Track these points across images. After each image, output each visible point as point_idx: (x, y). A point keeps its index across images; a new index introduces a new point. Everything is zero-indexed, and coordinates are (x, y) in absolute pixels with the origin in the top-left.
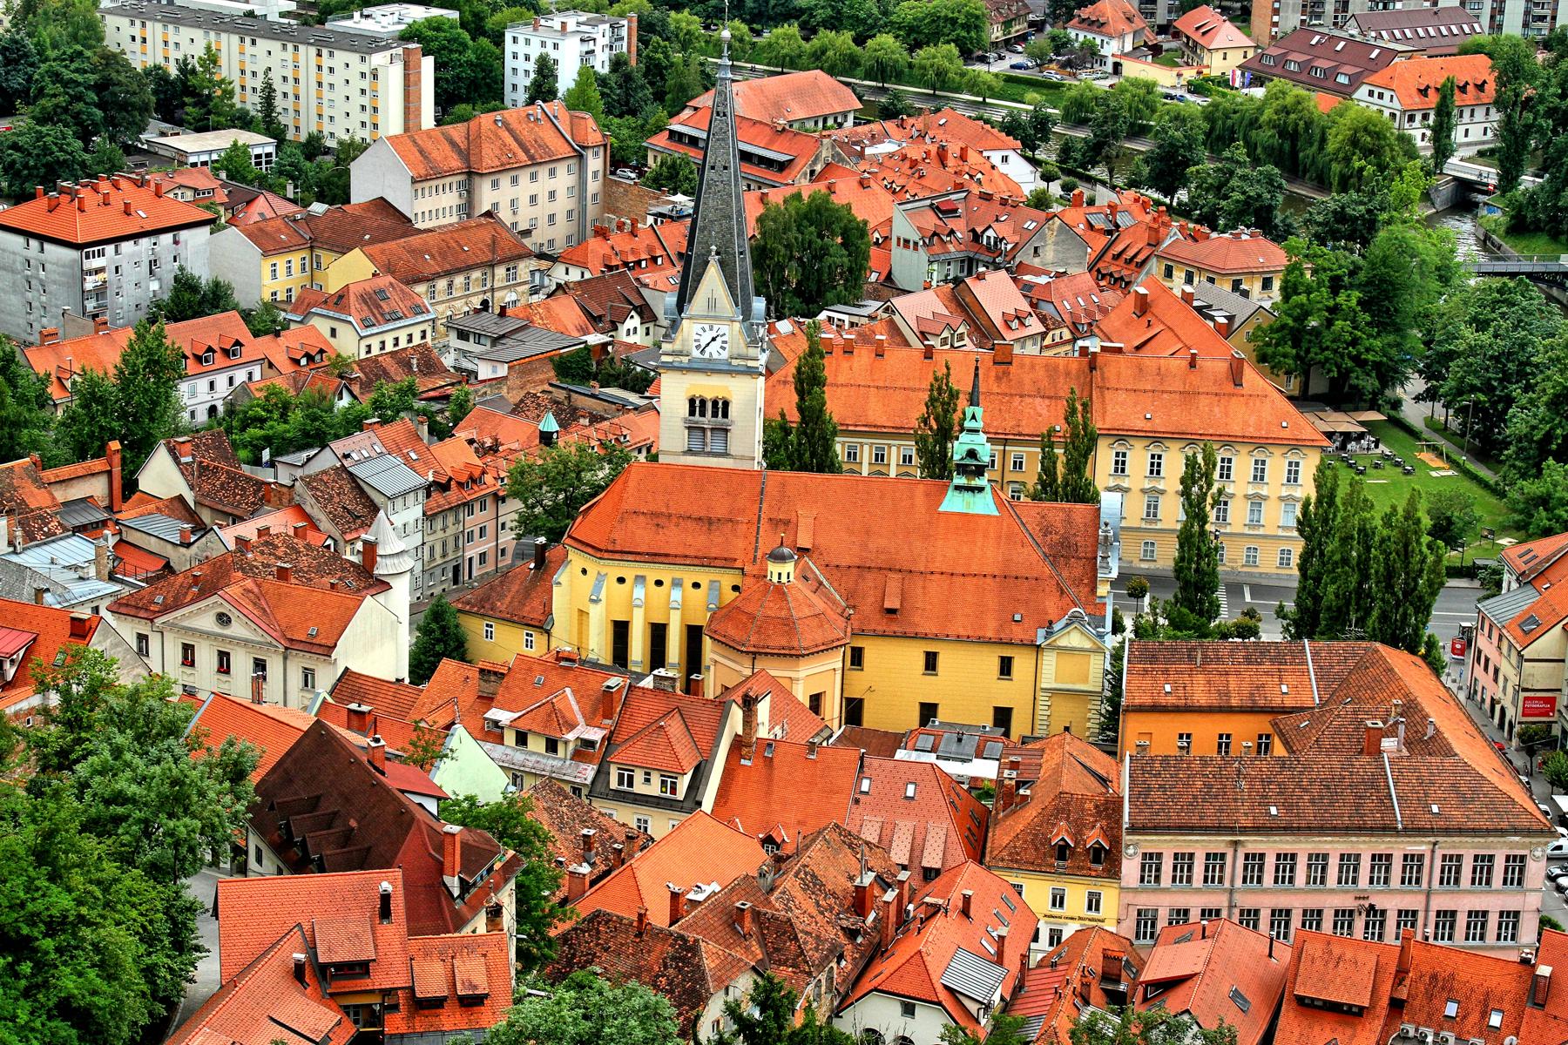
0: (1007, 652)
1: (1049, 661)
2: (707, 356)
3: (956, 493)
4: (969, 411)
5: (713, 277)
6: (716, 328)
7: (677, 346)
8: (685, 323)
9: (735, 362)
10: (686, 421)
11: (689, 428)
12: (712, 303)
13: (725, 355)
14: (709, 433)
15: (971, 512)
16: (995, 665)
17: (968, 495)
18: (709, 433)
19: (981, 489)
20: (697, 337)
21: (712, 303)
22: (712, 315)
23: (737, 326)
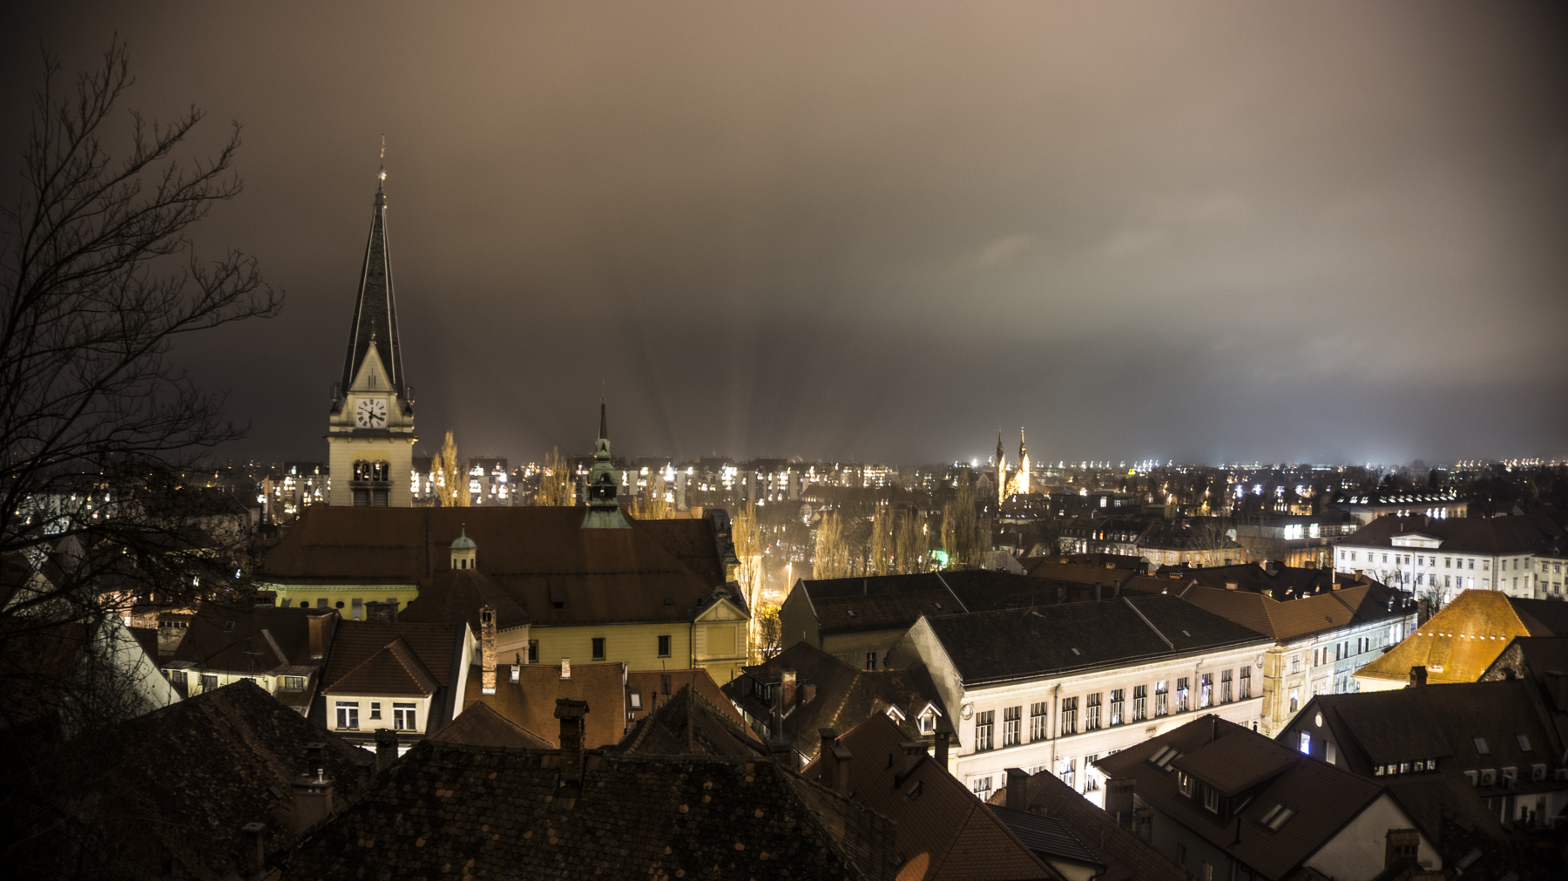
0: (664, 629)
1: (702, 635)
2: (368, 426)
3: (593, 513)
4: (600, 442)
5: (373, 352)
6: (375, 402)
7: (343, 417)
8: (350, 397)
9: (392, 430)
10: (351, 483)
11: (356, 491)
12: (372, 381)
13: (383, 424)
14: (372, 494)
15: (608, 527)
16: (656, 641)
17: (603, 515)
18: (372, 494)
19: (613, 508)
20: (360, 411)
21: (372, 381)
22: (372, 388)
23: (394, 398)
